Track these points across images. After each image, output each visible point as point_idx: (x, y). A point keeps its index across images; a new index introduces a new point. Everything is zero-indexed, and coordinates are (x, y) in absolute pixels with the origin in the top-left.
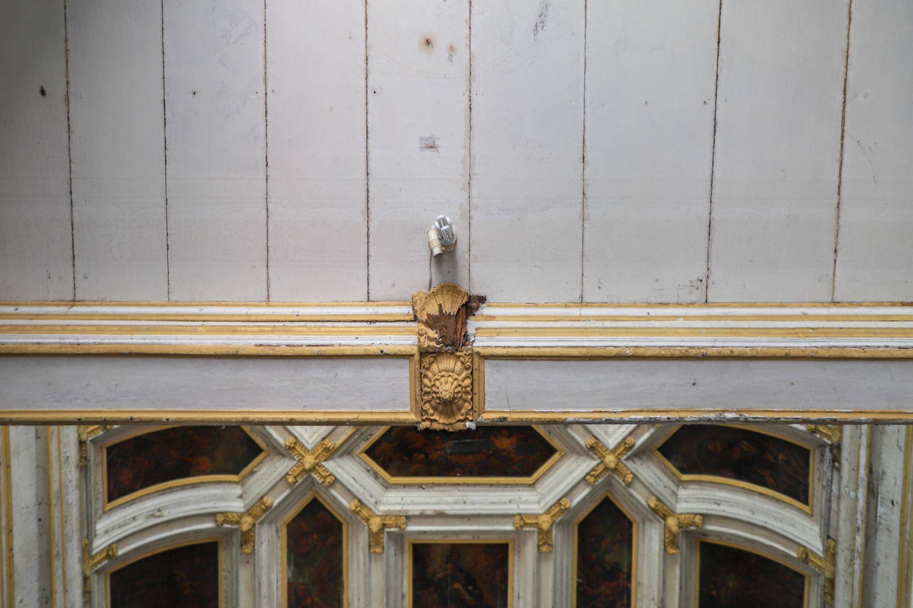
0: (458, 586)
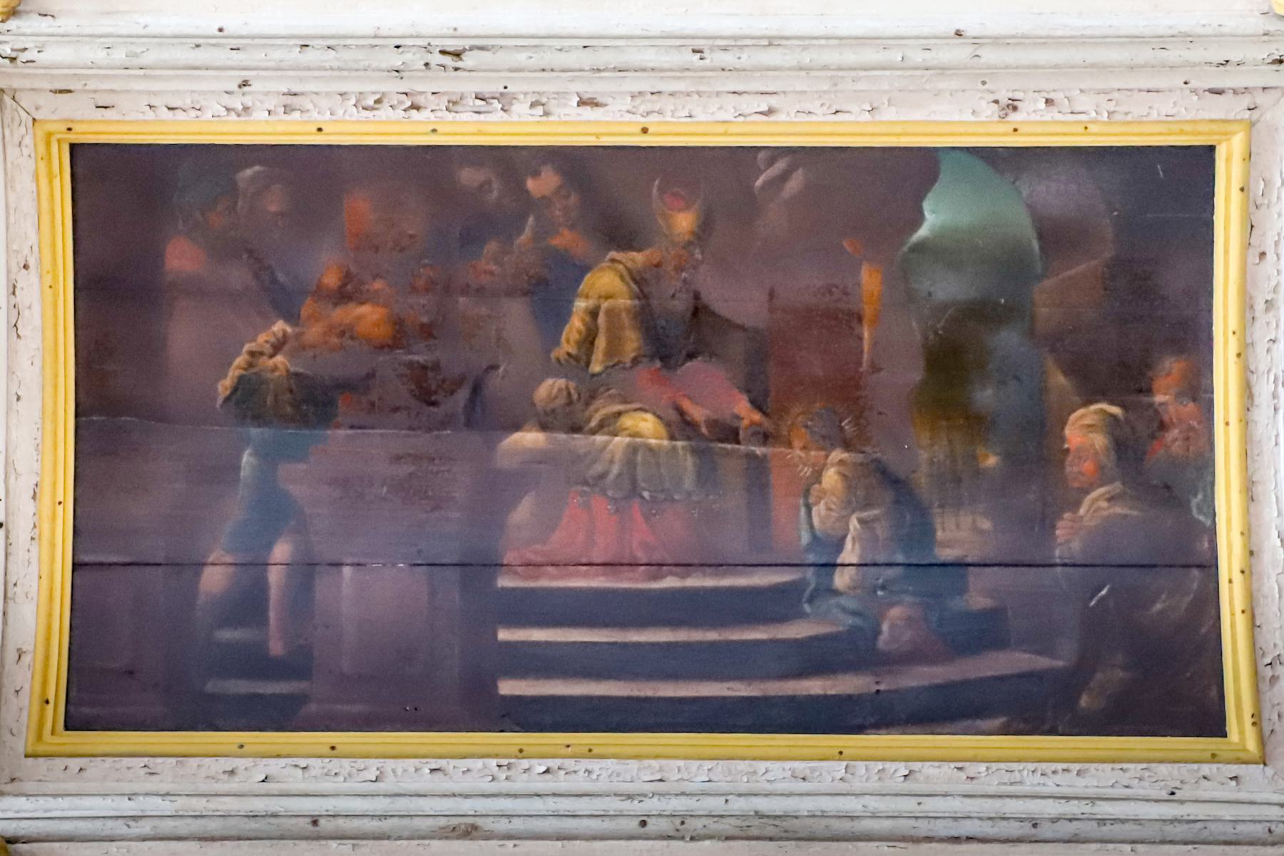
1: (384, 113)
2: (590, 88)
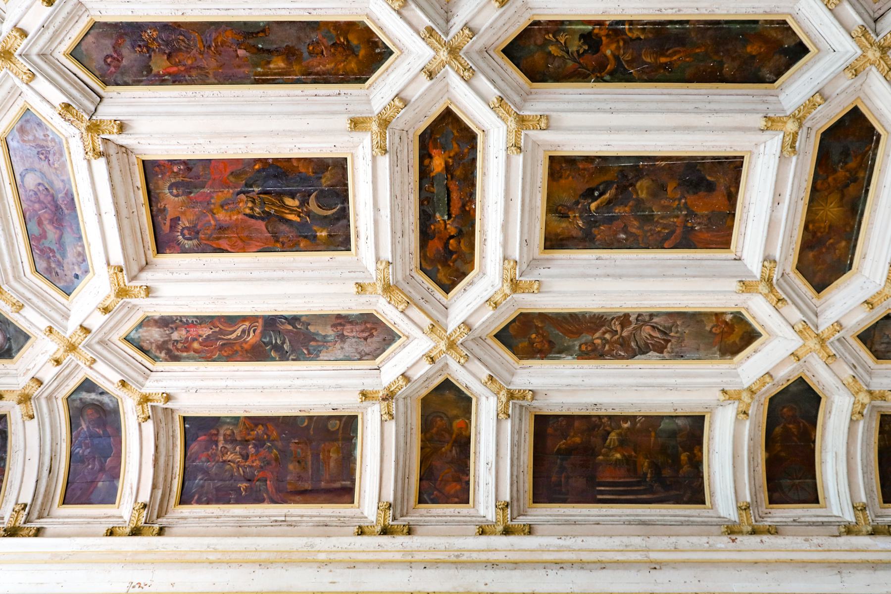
0: (593, 206)
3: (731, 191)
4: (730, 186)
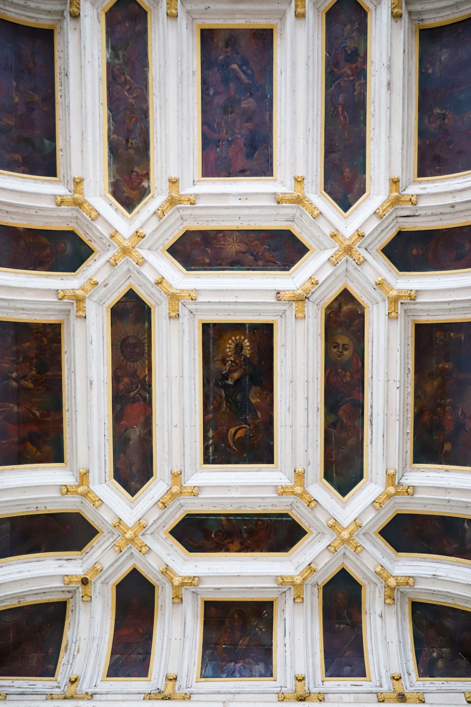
0: (235, 66)
1: (59, 70)
2: (63, 97)
3: (247, 171)
4: (250, 170)
